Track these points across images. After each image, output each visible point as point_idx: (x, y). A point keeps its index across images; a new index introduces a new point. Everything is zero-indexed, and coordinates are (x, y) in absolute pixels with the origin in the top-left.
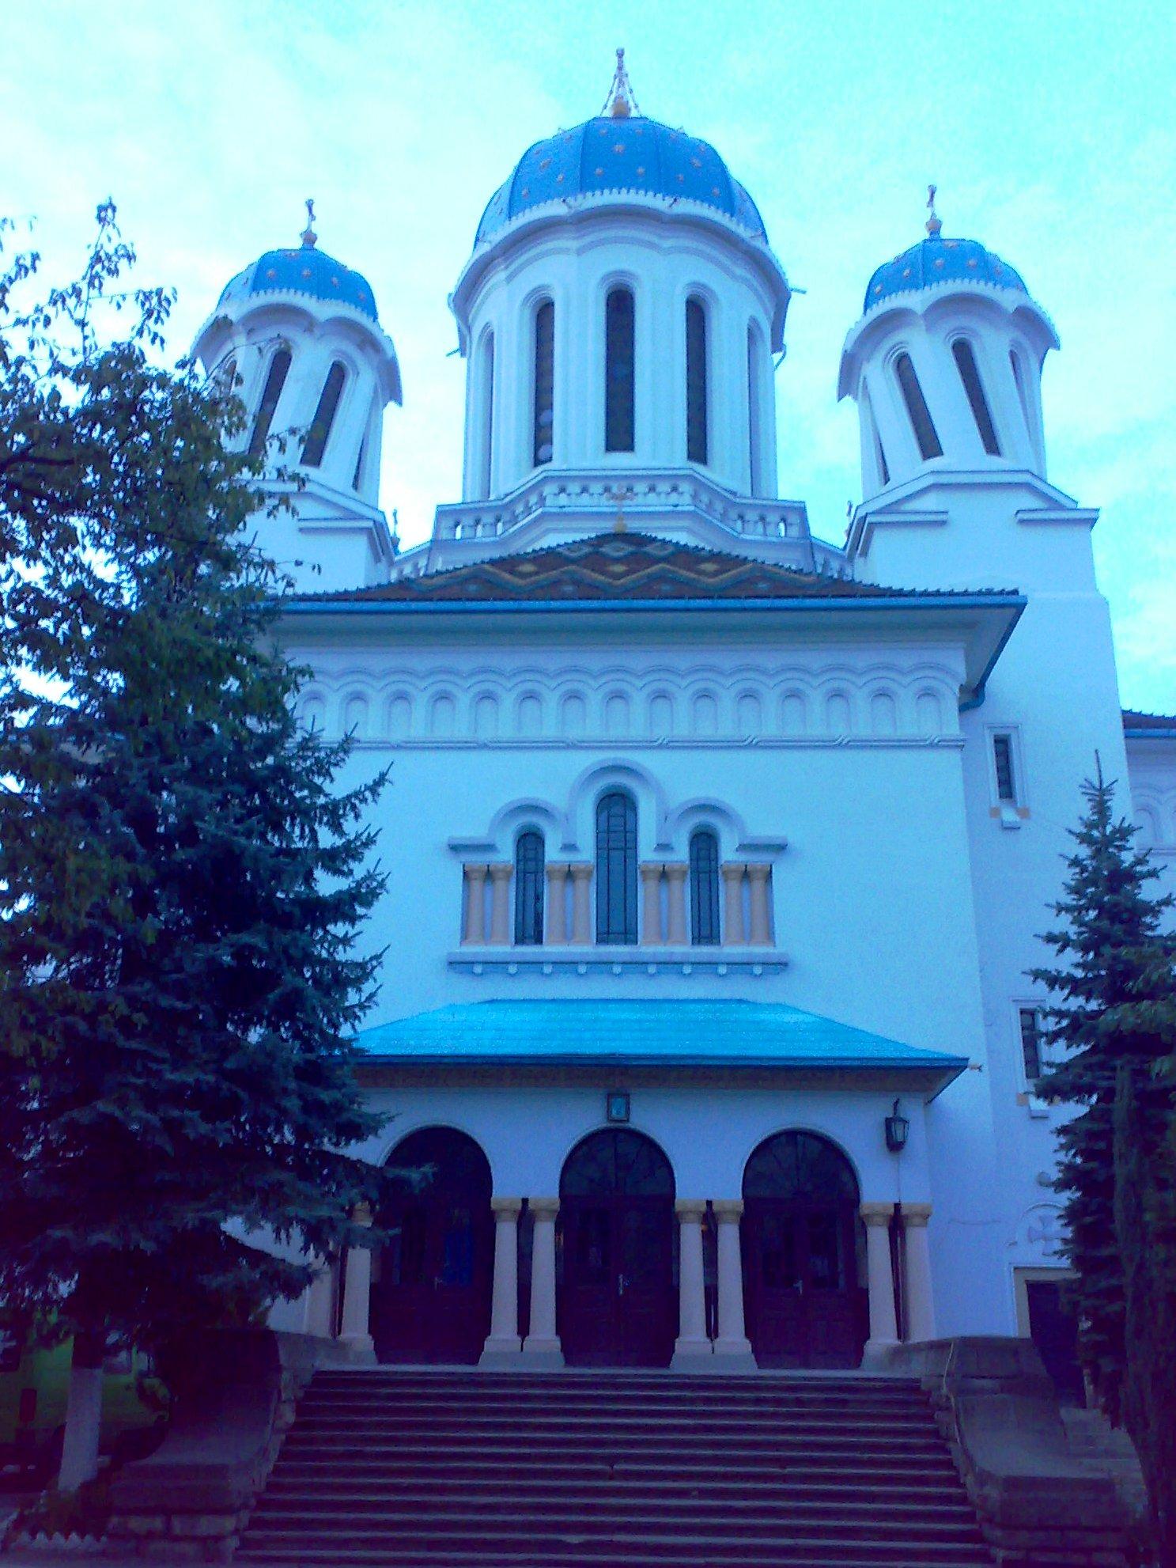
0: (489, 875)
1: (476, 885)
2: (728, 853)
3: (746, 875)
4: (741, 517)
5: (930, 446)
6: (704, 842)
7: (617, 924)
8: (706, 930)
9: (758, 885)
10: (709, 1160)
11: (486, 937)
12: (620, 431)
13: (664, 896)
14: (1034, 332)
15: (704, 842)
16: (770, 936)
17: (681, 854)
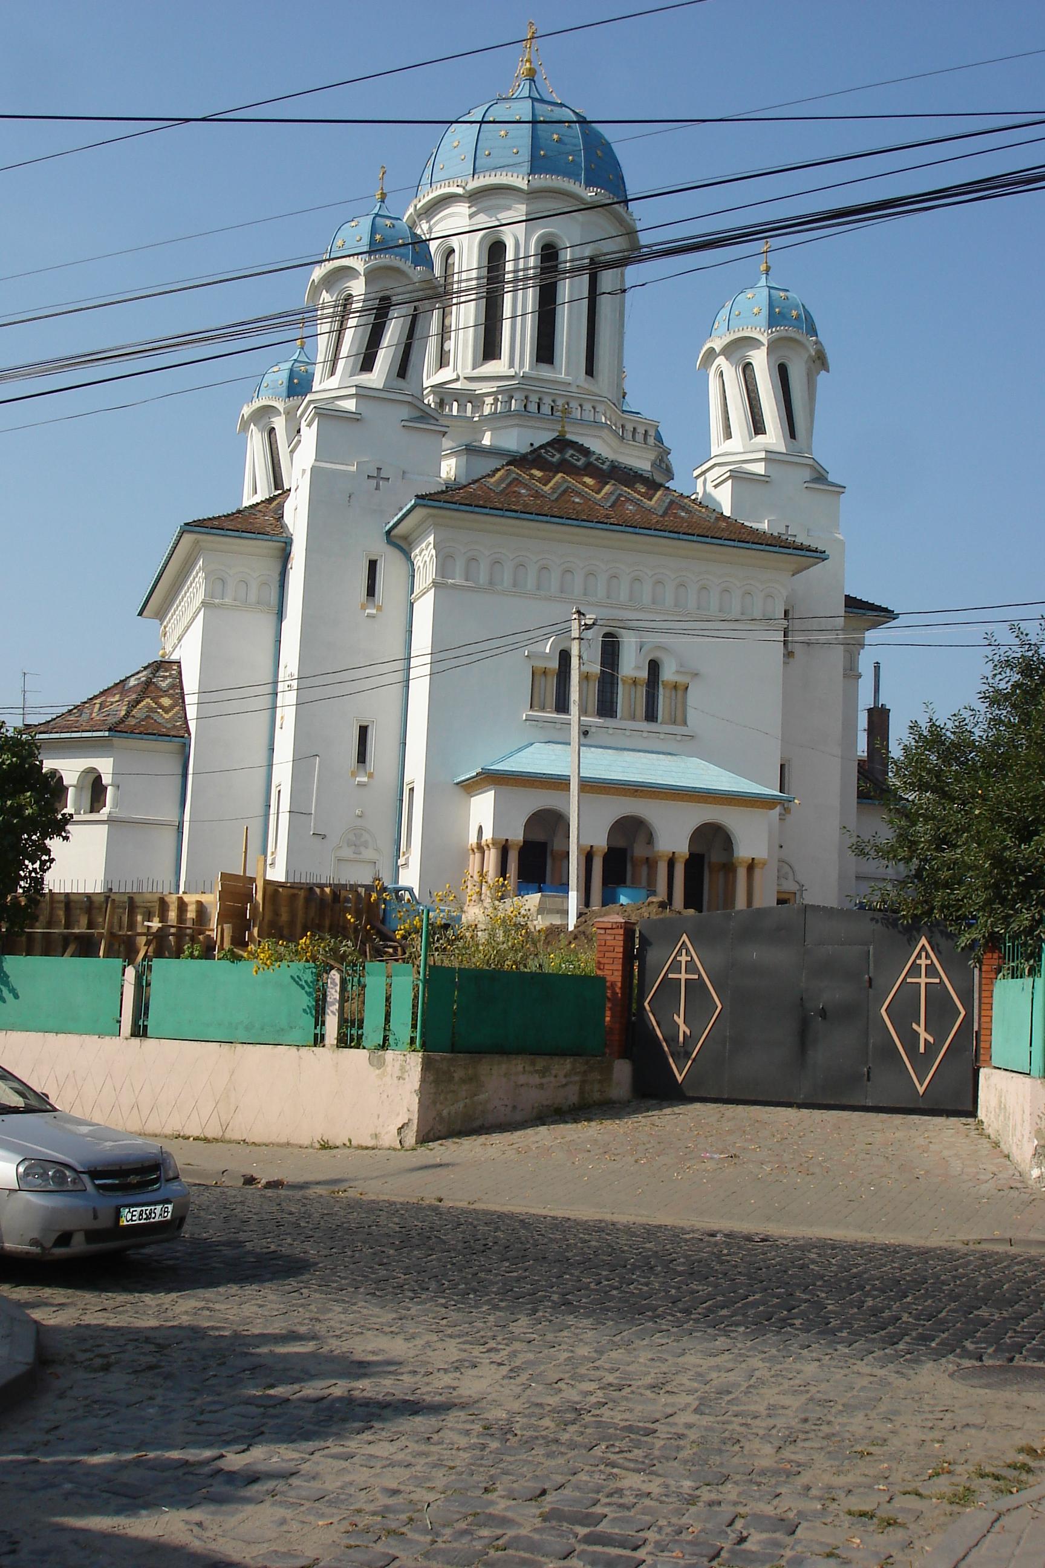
0: (545, 672)
1: (537, 678)
2: (668, 674)
3: (675, 687)
4: (623, 426)
5: (758, 427)
6: (654, 667)
7: (606, 708)
8: (651, 716)
9: (680, 693)
10: (673, 836)
11: (543, 709)
12: (545, 352)
13: (633, 692)
14: (820, 361)
15: (654, 667)
16: (685, 723)
17: (644, 674)
